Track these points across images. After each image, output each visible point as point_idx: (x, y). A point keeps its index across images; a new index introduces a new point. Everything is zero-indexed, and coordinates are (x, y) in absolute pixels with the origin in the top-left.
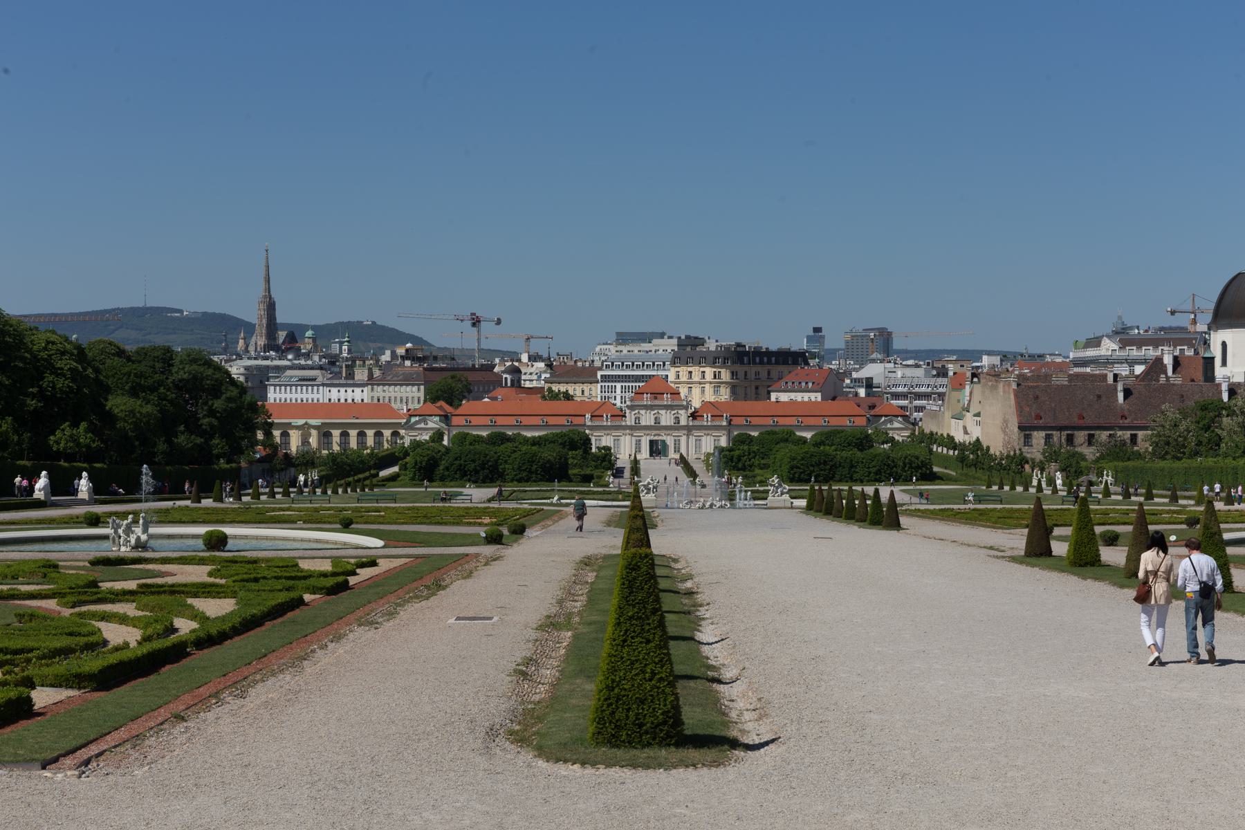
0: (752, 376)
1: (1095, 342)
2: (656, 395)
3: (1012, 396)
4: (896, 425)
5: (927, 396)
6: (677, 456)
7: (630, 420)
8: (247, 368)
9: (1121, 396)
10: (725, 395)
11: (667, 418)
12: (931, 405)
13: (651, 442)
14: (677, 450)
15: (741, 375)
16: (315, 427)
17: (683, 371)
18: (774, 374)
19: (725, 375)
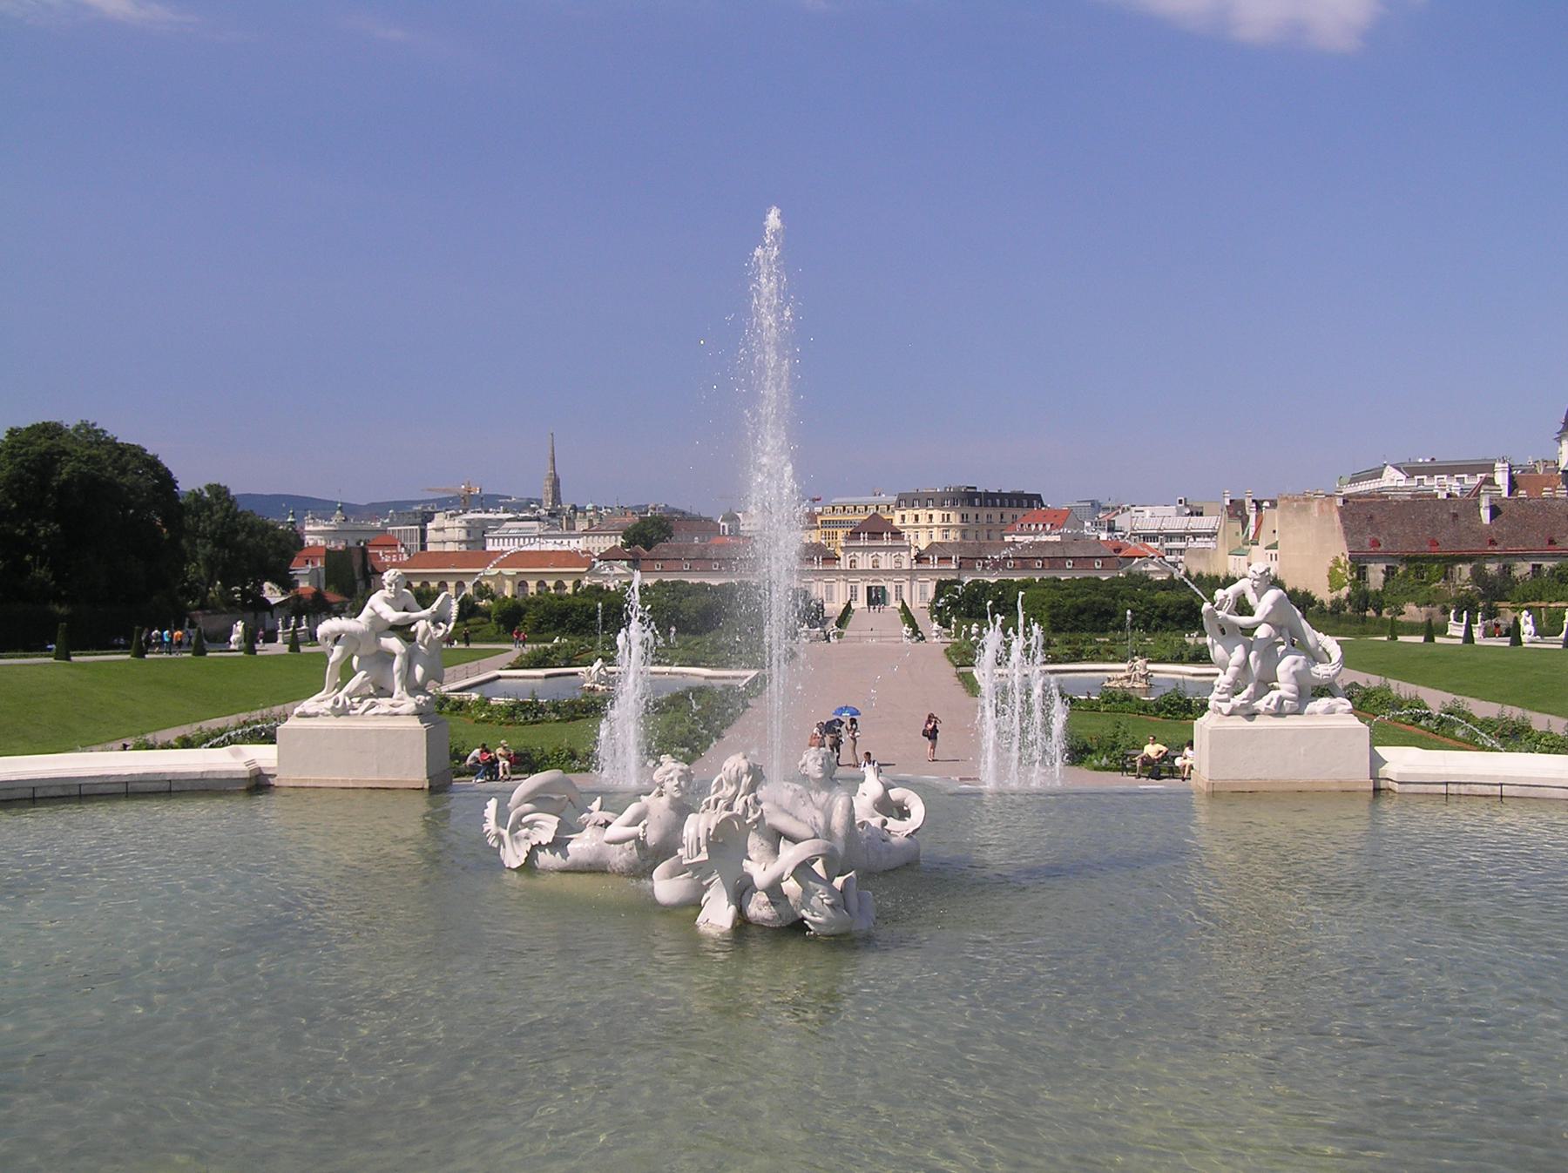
0: (983, 519)
1: (1378, 474)
2: (876, 535)
3: (1337, 517)
4: (1151, 567)
5: (1182, 537)
6: (899, 605)
7: (844, 564)
8: (468, 521)
9: (1485, 515)
10: (954, 536)
11: (886, 561)
12: (1199, 543)
13: (869, 588)
14: (899, 596)
15: (972, 518)
16: (509, 577)
17: (909, 514)
18: (1008, 518)
19: (955, 519)
